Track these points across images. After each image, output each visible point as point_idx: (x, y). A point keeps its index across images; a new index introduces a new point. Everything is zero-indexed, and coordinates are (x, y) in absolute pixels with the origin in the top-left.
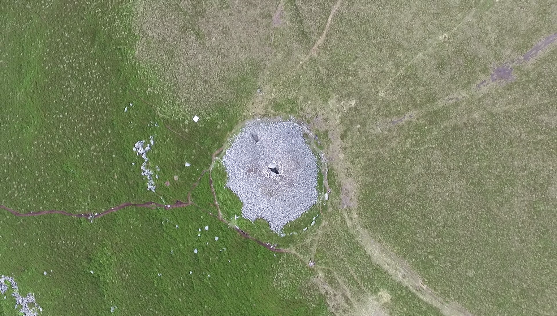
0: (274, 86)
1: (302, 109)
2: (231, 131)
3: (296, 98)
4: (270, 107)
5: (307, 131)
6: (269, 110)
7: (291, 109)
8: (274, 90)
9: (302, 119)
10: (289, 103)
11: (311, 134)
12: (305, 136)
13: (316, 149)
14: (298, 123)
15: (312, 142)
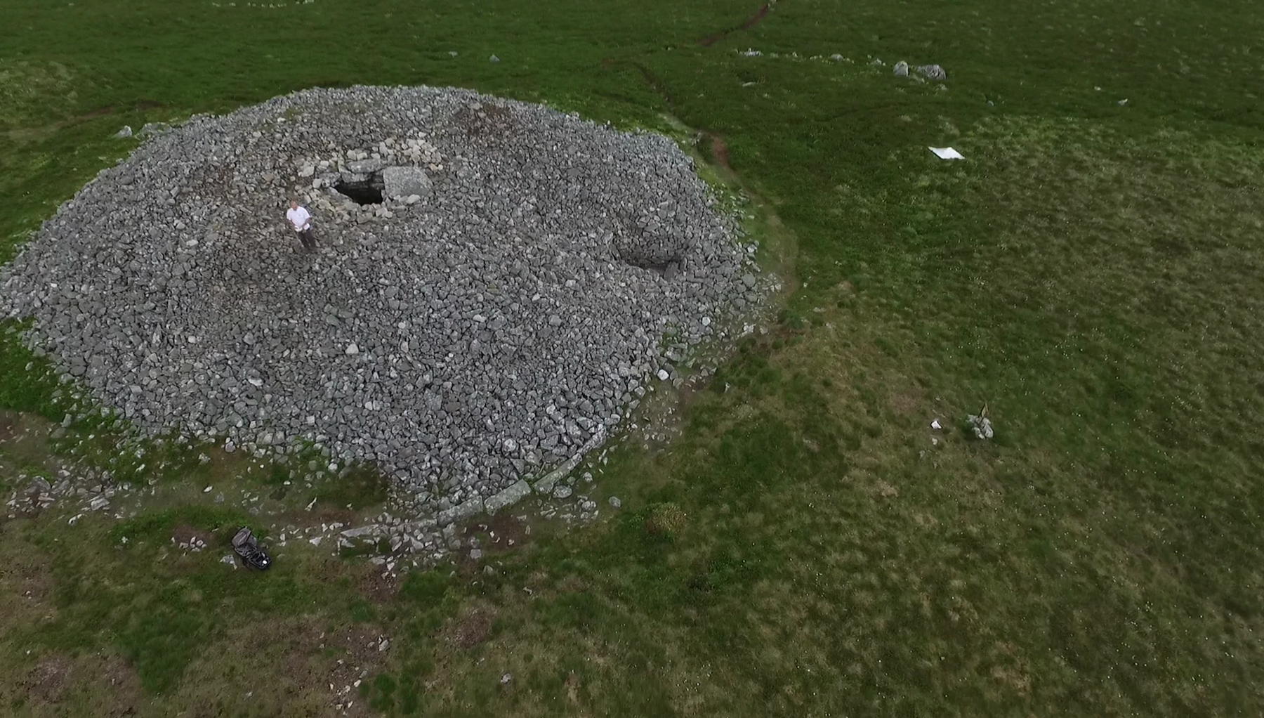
0: (968, 542)
1: (583, 614)
2: (783, 213)
3: (724, 644)
4: (789, 416)
5: (370, 530)
6: (773, 404)
7: (653, 541)
8: (922, 519)
9: (505, 555)
10: (721, 558)
11: (325, 536)
12: (365, 488)
13: (187, 490)
14: (503, 519)
15: (255, 501)
